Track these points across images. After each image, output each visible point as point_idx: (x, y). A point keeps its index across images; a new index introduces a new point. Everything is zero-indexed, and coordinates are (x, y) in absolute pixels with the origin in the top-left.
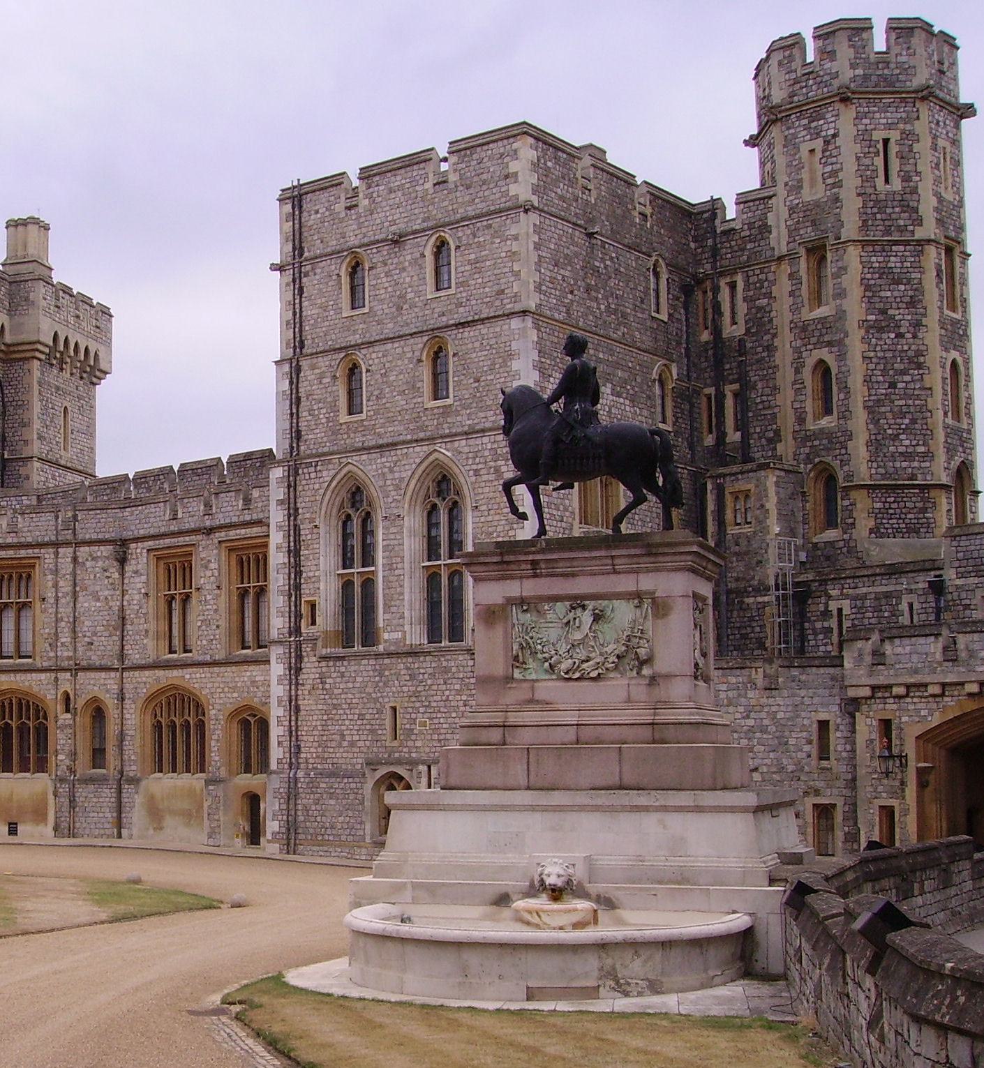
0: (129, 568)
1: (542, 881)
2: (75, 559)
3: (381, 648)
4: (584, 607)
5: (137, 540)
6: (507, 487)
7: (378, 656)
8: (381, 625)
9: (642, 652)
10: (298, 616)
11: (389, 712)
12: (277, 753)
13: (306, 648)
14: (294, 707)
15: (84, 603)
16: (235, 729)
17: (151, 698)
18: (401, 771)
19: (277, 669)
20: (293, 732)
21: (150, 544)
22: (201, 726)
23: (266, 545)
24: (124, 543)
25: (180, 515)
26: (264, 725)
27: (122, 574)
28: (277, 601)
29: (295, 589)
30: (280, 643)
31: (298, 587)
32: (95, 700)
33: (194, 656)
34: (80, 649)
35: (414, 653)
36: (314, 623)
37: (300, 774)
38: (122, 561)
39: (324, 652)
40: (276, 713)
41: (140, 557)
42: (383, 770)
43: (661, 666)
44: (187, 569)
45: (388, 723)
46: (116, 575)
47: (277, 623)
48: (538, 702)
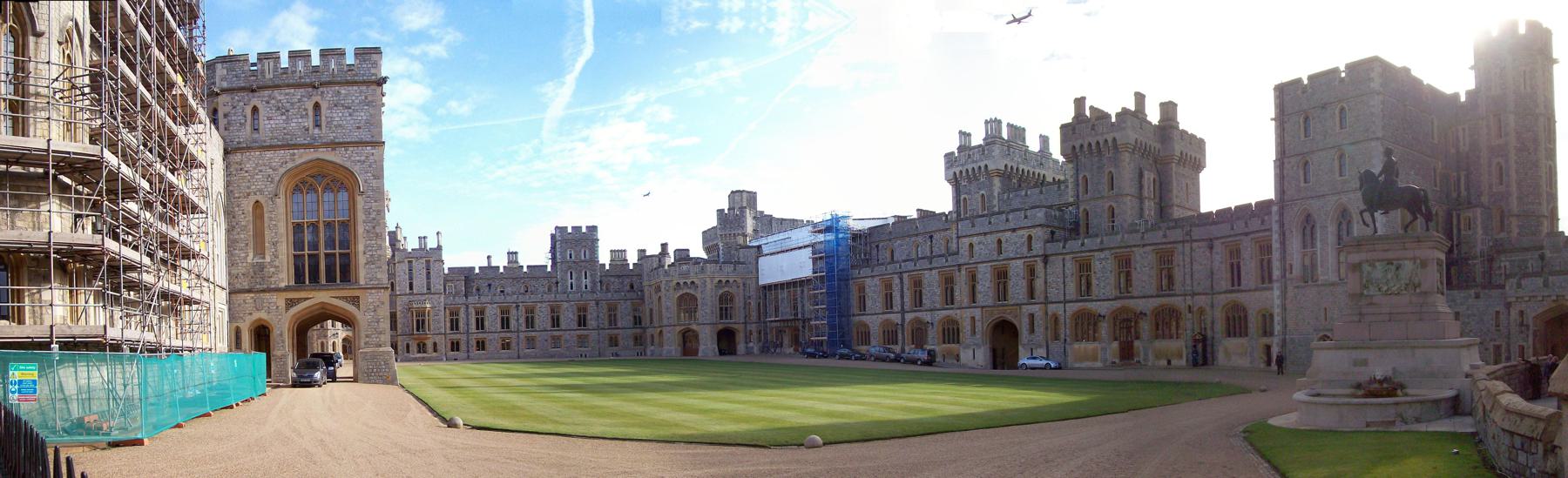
0: (1214, 251)
1: (1375, 378)
2: (1191, 248)
3: (1320, 282)
4: (1392, 264)
5: (1217, 238)
6: (1361, 213)
7: (1318, 285)
8: (1319, 273)
9: (1416, 281)
10: (1285, 270)
11: (1323, 310)
12: (1277, 328)
13: (1289, 282)
14: (1284, 308)
15: (1196, 267)
16: (1260, 318)
17: (1224, 306)
18: (1329, 334)
19: (1277, 293)
20: (1284, 320)
21: (1223, 240)
22: (1246, 316)
23: (1271, 240)
24: (1211, 240)
25: (1235, 227)
26: (1272, 316)
27: (1211, 253)
28: (1276, 264)
29: (1283, 259)
30: (1277, 281)
31: (1284, 257)
32: (1201, 308)
33: (1242, 288)
34: (1195, 284)
35: (1333, 284)
36: (1291, 273)
37: (1287, 337)
38: (1211, 248)
39: (1297, 285)
40: (1277, 311)
41: (1217, 244)
42: (1321, 334)
43: (1424, 287)
44: (1238, 251)
45: (1323, 314)
46: (1209, 254)
47: (1276, 273)
48: (1374, 304)
